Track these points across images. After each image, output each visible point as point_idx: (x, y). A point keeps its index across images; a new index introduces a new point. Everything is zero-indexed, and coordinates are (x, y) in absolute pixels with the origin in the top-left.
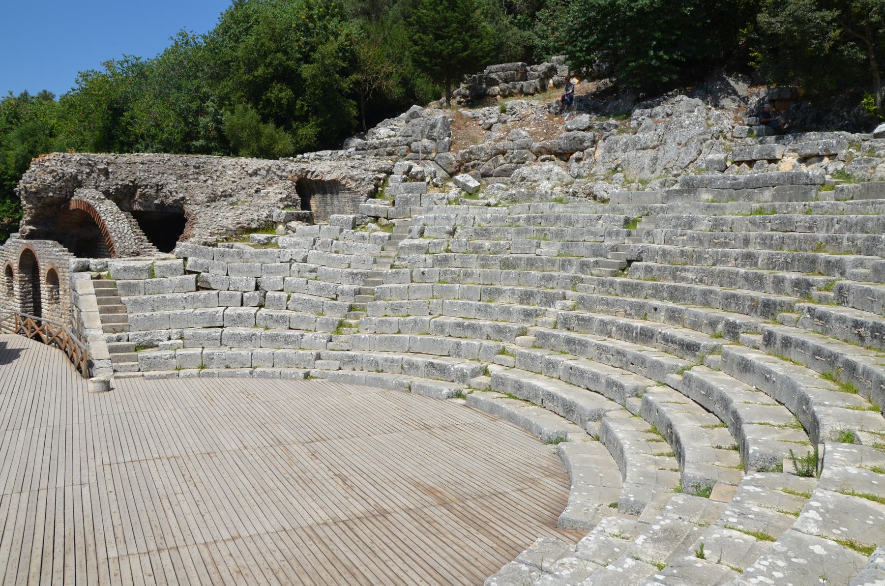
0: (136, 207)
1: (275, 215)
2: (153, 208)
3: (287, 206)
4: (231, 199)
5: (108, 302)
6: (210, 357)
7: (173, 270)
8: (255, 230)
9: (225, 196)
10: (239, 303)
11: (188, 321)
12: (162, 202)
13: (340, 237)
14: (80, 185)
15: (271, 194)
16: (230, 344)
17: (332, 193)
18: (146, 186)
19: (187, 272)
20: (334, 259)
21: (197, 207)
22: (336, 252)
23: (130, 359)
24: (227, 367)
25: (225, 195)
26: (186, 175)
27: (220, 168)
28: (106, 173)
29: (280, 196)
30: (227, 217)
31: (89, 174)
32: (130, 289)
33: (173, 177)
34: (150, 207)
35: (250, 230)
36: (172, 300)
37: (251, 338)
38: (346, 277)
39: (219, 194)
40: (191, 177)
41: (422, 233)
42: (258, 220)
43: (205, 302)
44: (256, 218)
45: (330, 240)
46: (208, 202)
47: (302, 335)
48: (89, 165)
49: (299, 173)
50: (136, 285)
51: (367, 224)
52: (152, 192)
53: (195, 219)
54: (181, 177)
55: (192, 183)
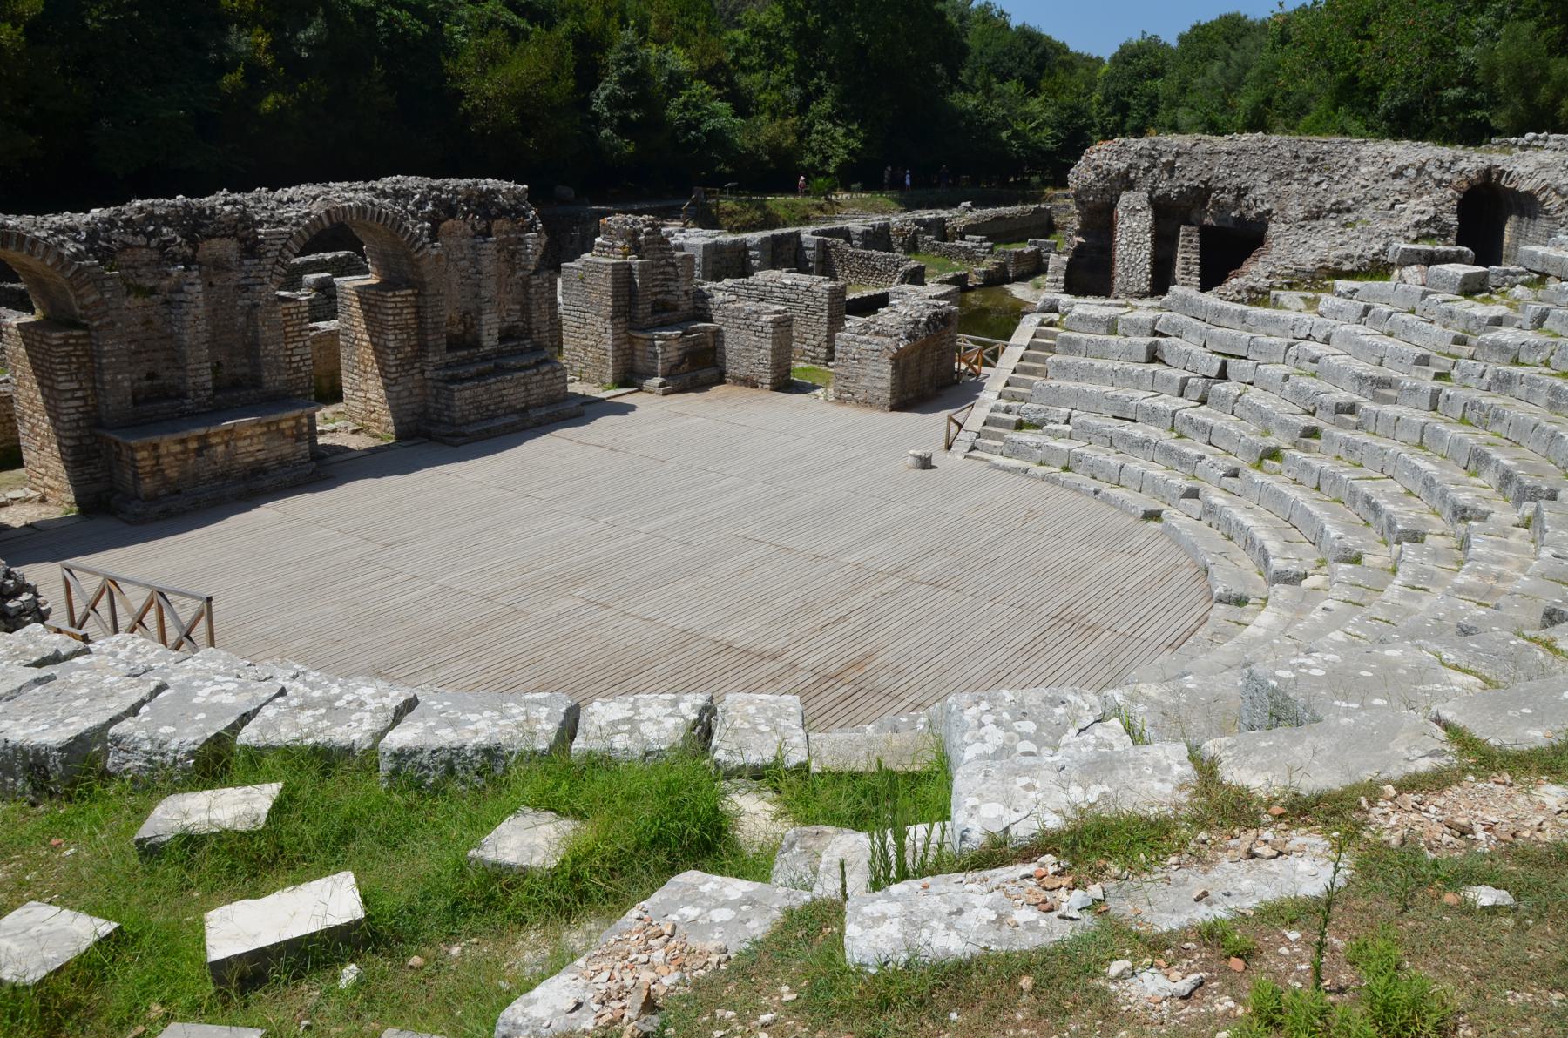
0: (1208, 220)
1: (1391, 250)
2: (1230, 224)
3: (1427, 237)
4: (1347, 216)
5: (1035, 359)
6: (1079, 458)
7: (1136, 327)
8: (1350, 275)
9: (1339, 211)
10: (1176, 392)
11: (1093, 403)
12: (1242, 214)
13: (1419, 307)
14: (1131, 186)
15: (1408, 212)
16: (1121, 447)
17: (1521, 215)
18: (1223, 190)
19: (1156, 333)
20: (1362, 345)
21: (1284, 227)
22: (1390, 335)
23: (1000, 437)
24: (1094, 477)
25: (1338, 209)
26: (1290, 174)
27: (1351, 162)
28: (1170, 168)
29: (1417, 217)
30: (1321, 245)
31: (1147, 170)
32: (1071, 346)
33: (1266, 177)
34: (1226, 220)
35: (1339, 274)
36: (1100, 370)
37: (1144, 444)
38: (1353, 380)
39: (1328, 206)
40: (1297, 176)
41: (1539, 321)
42: (1360, 257)
43: (1138, 382)
44: (1359, 252)
45: (1387, 309)
46: (1304, 219)
47: (1201, 458)
48: (1151, 156)
49: (1473, 176)
50: (1077, 342)
51: (1513, 286)
52: (1229, 198)
53: (1269, 248)
54: (1280, 176)
55: (1295, 186)
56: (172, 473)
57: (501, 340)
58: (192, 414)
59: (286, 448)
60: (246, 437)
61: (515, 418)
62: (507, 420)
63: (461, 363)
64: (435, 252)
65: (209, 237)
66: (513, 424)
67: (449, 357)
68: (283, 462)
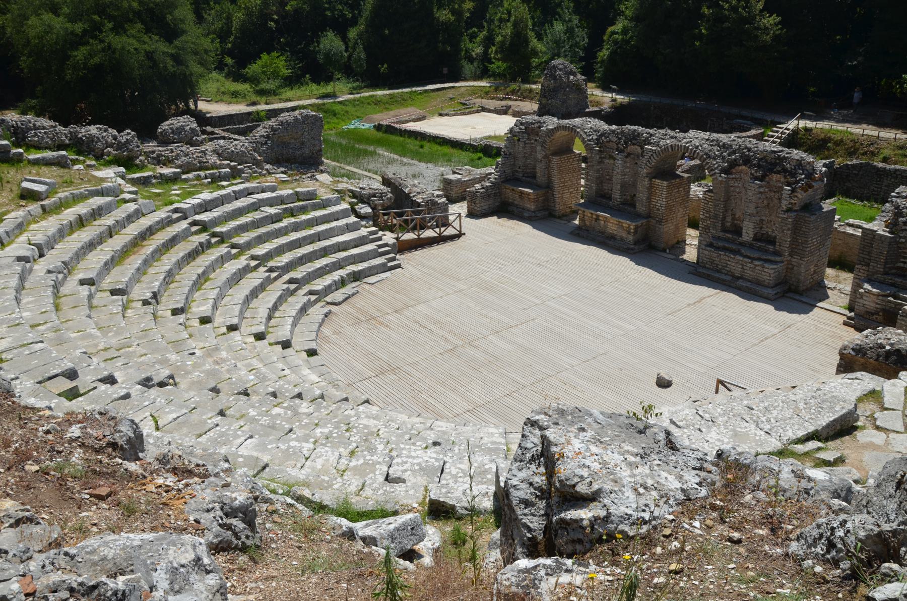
56: (588, 223)
57: (756, 238)
58: (611, 208)
59: (624, 235)
60: (611, 223)
61: (729, 278)
62: (724, 277)
63: (727, 240)
64: (720, 179)
65: (634, 144)
66: (725, 280)
67: (721, 234)
68: (622, 239)
